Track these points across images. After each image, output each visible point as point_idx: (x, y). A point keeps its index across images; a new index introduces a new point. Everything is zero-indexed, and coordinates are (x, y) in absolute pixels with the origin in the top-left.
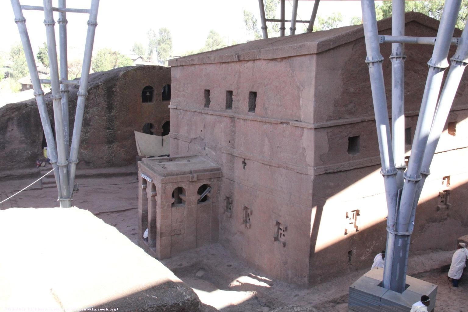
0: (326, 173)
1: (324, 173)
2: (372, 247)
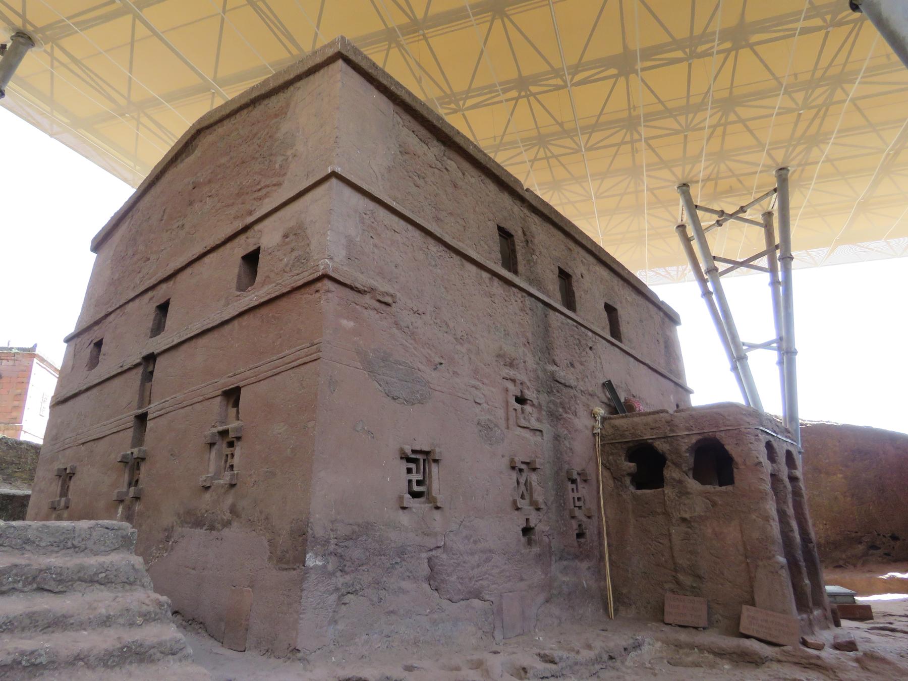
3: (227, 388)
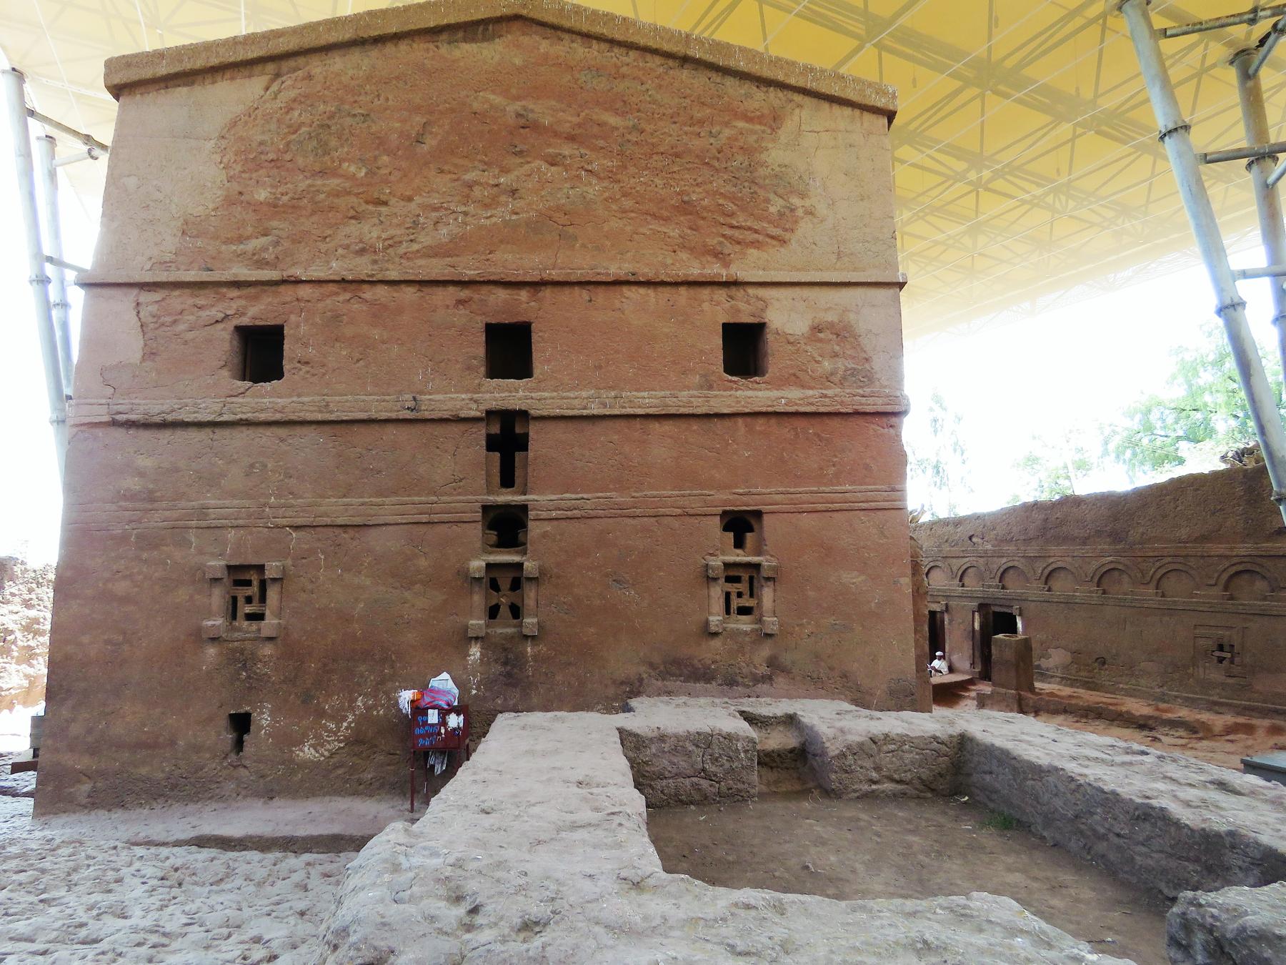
0: (114, 423)
1: (106, 418)
2: (351, 718)
3: (736, 509)
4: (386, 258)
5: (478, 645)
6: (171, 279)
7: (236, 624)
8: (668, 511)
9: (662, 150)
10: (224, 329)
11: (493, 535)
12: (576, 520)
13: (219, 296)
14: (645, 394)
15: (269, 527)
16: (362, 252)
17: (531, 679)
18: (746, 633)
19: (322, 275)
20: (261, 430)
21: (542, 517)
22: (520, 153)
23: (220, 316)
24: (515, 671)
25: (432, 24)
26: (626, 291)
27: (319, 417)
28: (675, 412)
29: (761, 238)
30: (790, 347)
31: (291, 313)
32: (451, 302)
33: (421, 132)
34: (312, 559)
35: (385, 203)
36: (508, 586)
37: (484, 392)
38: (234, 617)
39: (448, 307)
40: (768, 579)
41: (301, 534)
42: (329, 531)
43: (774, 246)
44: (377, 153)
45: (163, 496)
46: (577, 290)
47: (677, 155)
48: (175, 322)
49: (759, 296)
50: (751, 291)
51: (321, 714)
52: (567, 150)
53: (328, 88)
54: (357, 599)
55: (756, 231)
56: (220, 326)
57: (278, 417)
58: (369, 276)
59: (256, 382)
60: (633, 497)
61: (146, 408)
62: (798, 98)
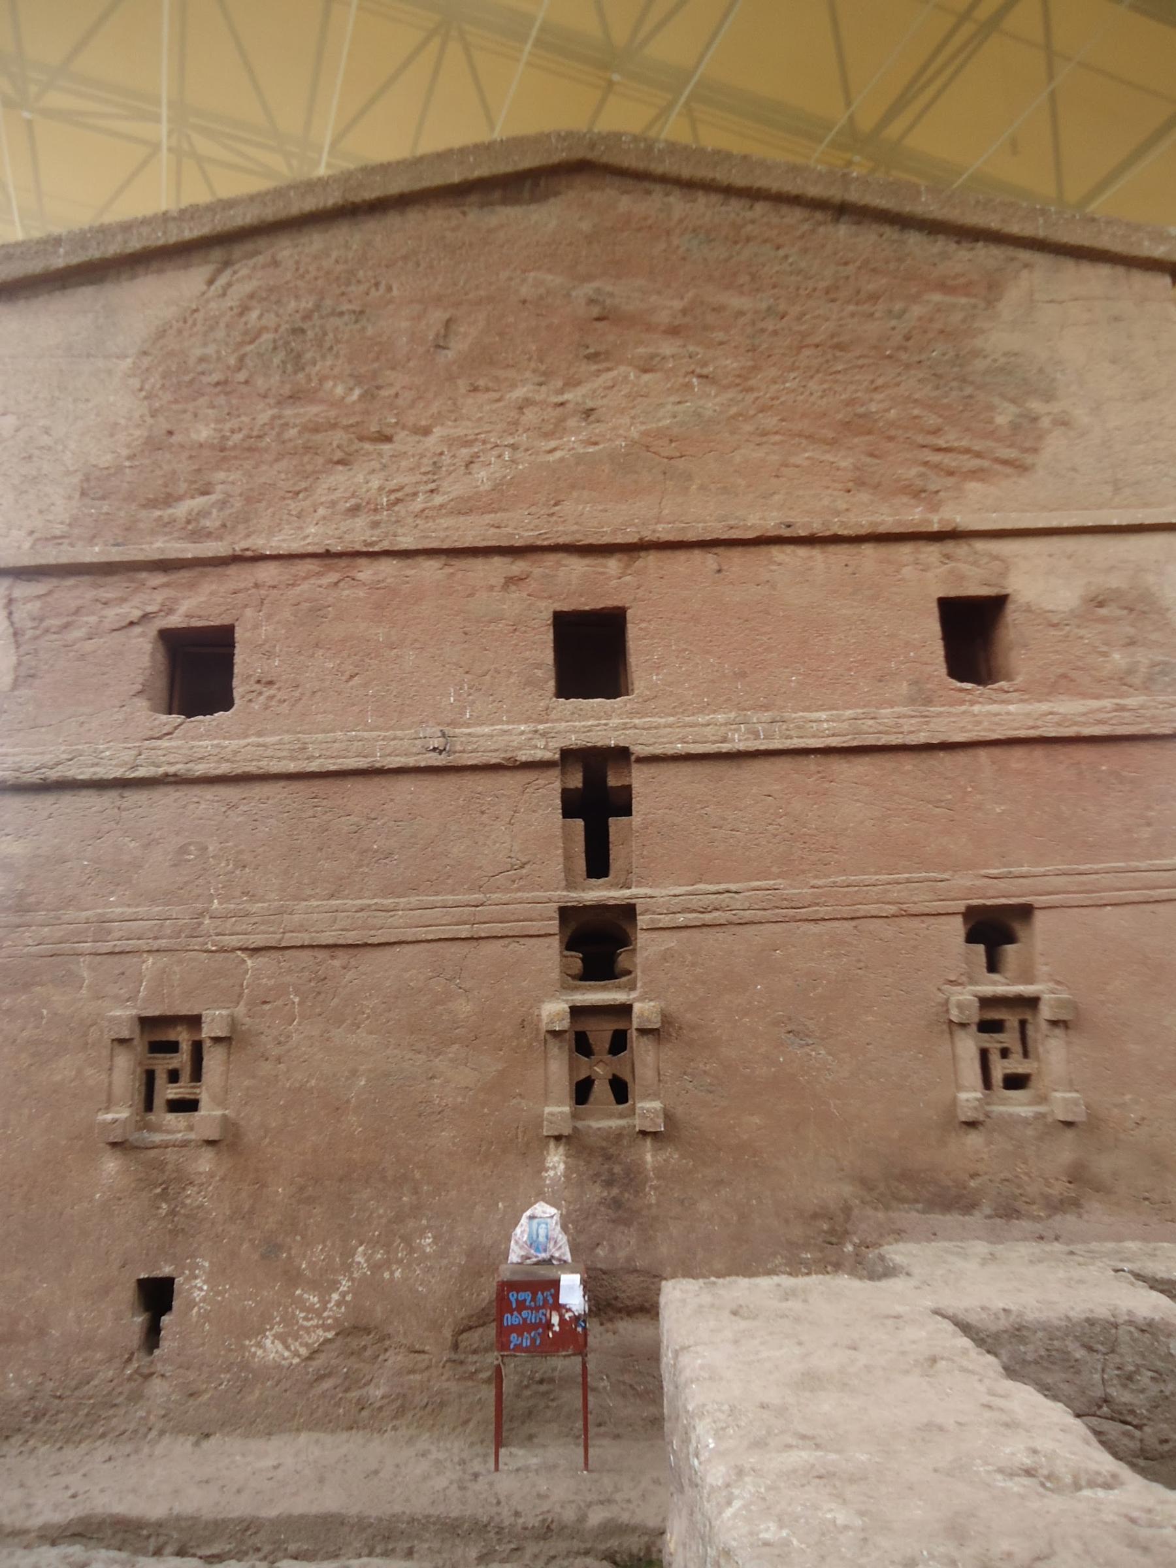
2: (345, 1285)
3: (989, 902)
4: (393, 519)
5: (561, 1150)
6: (64, 560)
7: (152, 1117)
8: (872, 909)
9: (817, 340)
10: (143, 635)
11: (576, 962)
12: (718, 929)
13: (133, 585)
14: (823, 715)
15: (212, 952)
16: (355, 510)
17: (654, 1211)
18: (1026, 1122)
19: (296, 547)
20: (196, 791)
21: (661, 925)
22: (593, 357)
23: (136, 614)
24: (626, 1195)
25: (456, 178)
26: (778, 553)
27: (292, 767)
28: (873, 742)
29: (985, 463)
30: (1053, 632)
31: (246, 606)
32: (497, 580)
33: (442, 331)
34: (279, 1003)
35: (388, 439)
36: (607, 1046)
37: (557, 721)
38: (149, 1106)
39: (491, 588)
40: (1054, 1023)
41: (262, 960)
42: (306, 956)
43: (1007, 476)
44: (376, 365)
45: (38, 903)
46: (697, 555)
47: (840, 347)
48: (66, 626)
49: (995, 553)
50: (980, 545)
51: (293, 1278)
52: (668, 347)
53: (302, 277)
54: (354, 1073)
55: (978, 455)
56: (137, 630)
57: (224, 769)
58: (367, 544)
59: (189, 715)
60: (813, 887)
61: (17, 759)
62: (1025, 255)
